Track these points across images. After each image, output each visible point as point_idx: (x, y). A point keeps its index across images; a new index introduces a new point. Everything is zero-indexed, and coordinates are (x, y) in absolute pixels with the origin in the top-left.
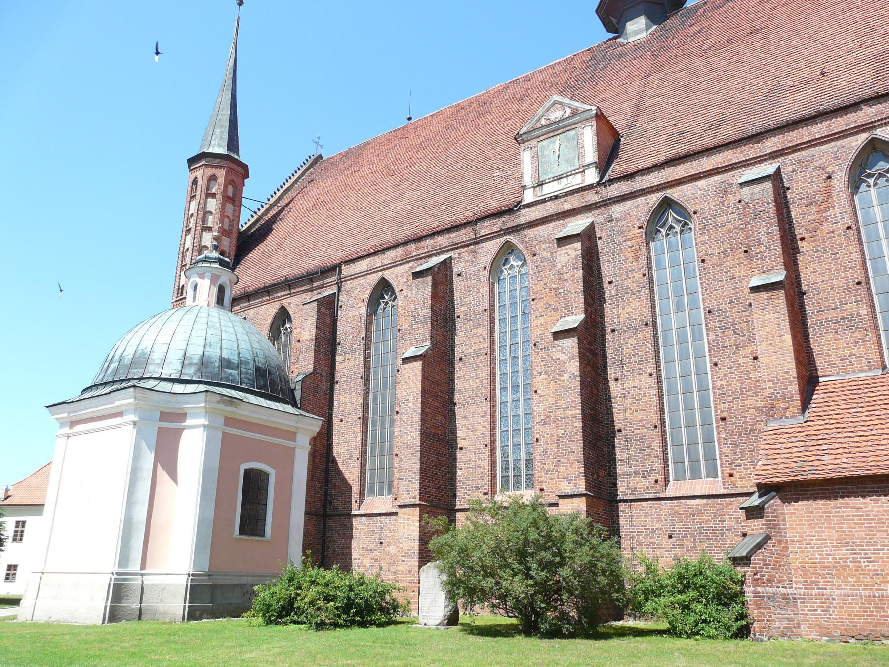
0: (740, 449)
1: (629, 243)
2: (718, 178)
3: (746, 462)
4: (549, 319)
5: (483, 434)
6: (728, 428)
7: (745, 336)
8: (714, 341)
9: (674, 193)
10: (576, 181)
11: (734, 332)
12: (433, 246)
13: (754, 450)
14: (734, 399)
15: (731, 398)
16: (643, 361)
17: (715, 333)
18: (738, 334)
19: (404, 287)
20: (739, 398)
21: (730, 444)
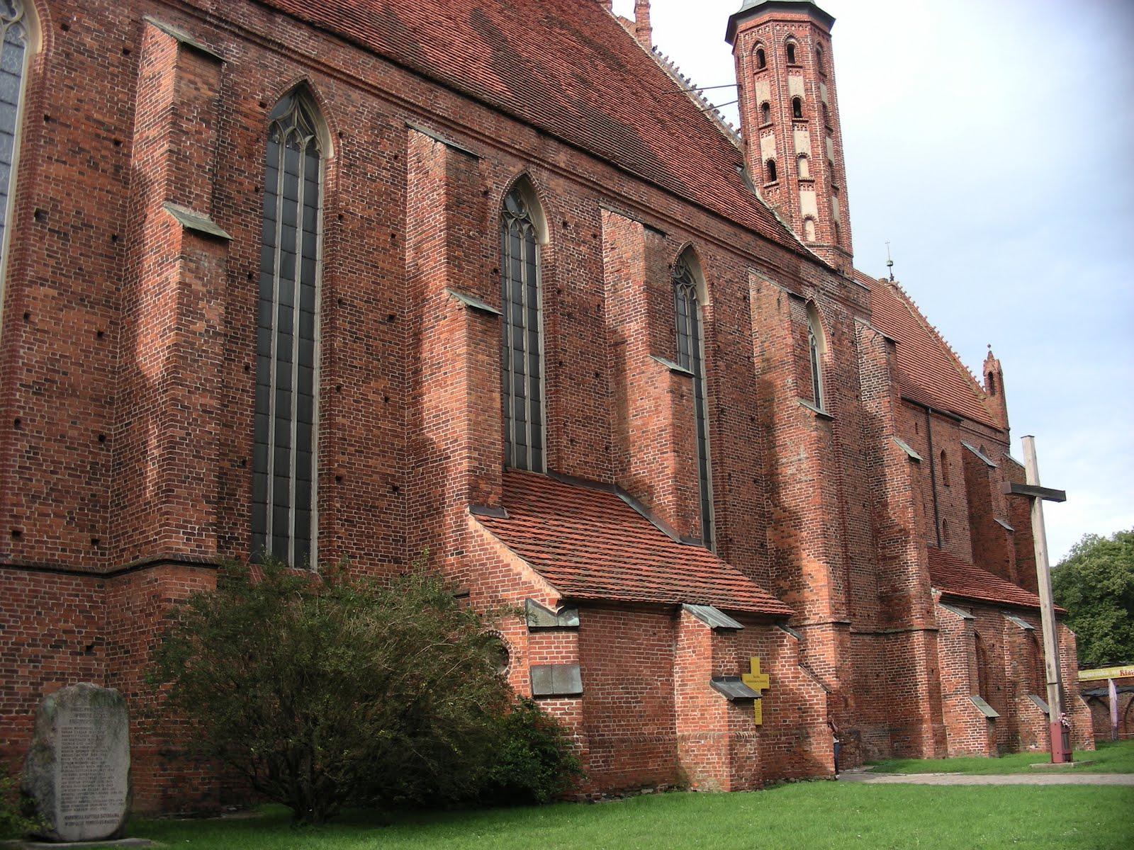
0: (357, 531)
1: (244, 121)
2: (375, 103)
3: (363, 552)
4: (76, 176)
6: (345, 494)
7: (379, 360)
8: (340, 350)
9: (321, 86)
11: (367, 349)
13: (373, 537)
14: (356, 451)
15: (353, 449)
16: (238, 338)
17: (344, 339)
18: (372, 354)
20: (362, 452)
21: (346, 520)
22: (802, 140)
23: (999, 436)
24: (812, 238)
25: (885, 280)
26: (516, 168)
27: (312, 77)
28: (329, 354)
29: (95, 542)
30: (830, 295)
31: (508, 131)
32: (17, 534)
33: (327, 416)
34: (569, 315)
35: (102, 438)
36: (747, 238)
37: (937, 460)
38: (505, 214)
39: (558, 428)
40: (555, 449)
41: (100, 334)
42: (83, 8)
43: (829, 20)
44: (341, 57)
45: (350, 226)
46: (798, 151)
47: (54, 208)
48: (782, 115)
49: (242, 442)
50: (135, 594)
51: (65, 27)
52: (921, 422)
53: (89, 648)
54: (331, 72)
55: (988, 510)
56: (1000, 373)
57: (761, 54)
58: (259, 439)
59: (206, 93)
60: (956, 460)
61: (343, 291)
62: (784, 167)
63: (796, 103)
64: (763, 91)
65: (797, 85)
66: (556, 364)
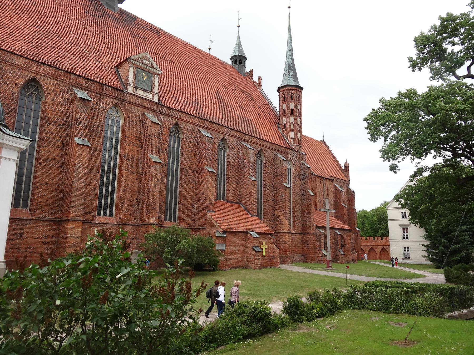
1: (164, 133)
2: (192, 125)
4: (131, 148)
5: (95, 188)
9: (180, 123)
10: (150, 96)
12: (76, 82)
19: (52, 93)
22: (292, 119)
23: (347, 182)
24: (292, 143)
25: (321, 141)
26: (222, 136)
27: (178, 122)
28: (181, 180)
29: (135, 219)
30: (295, 157)
31: (220, 129)
32: (120, 218)
33: (180, 192)
34: (232, 167)
35: (136, 199)
37: (326, 190)
38: (219, 146)
39: (228, 192)
40: (227, 196)
41: (136, 179)
42: (132, 113)
43: (302, 89)
44: (184, 117)
45: (186, 153)
46: (291, 122)
48: (288, 113)
49: (164, 198)
50: (143, 229)
51: (128, 117)
52: (322, 181)
53: (133, 239)
54: (182, 120)
56: (348, 166)
57: (285, 97)
58: (167, 197)
59: (157, 131)
60: (331, 189)
61: (184, 166)
62: (288, 125)
63: (292, 110)
64: (284, 107)
65: (292, 106)
66: (228, 178)
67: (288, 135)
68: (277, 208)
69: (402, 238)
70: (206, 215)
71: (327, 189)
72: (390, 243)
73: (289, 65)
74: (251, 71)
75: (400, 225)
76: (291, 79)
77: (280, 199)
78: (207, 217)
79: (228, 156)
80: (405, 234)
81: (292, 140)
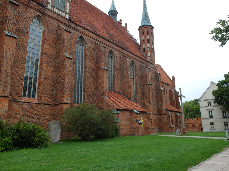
1: (73, 41)
2: (91, 39)
4: (50, 48)
5: (21, 75)
9: (84, 36)
10: (63, 14)
22: (148, 45)
23: (174, 87)
24: (149, 59)
25: (158, 64)
26: (110, 49)
27: (83, 35)
28: (85, 75)
29: (52, 100)
30: (152, 67)
31: (109, 44)
32: (41, 99)
33: (84, 83)
34: (117, 70)
35: (53, 86)
36: (141, 59)
37: (165, 90)
38: (109, 55)
39: (115, 85)
40: (114, 88)
41: (53, 71)
42: (50, 23)
43: (153, 28)
44: (86, 32)
45: (88, 56)
46: (148, 47)
47: (47, 53)
48: (146, 41)
49: (73, 87)
50: (59, 108)
51: (48, 26)
52: (163, 85)
53: (51, 115)
54: (85, 34)
55: (172, 97)
56: (174, 78)
57: (143, 32)
58: (75, 86)
59: (69, 37)
60: (168, 90)
61: (87, 66)
62: (146, 49)
63: (148, 40)
64: (143, 38)
65: (148, 37)
66: (115, 76)
67: (146, 55)
68: (144, 97)
69: (209, 117)
70: (103, 99)
71: (166, 90)
72: (202, 120)
73: (145, 14)
74: (121, 20)
75: (207, 110)
76: (147, 22)
77: (146, 92)
78: (104, 100)
79: (114, 62)
80: (211, 115)
81: (149, 58)
